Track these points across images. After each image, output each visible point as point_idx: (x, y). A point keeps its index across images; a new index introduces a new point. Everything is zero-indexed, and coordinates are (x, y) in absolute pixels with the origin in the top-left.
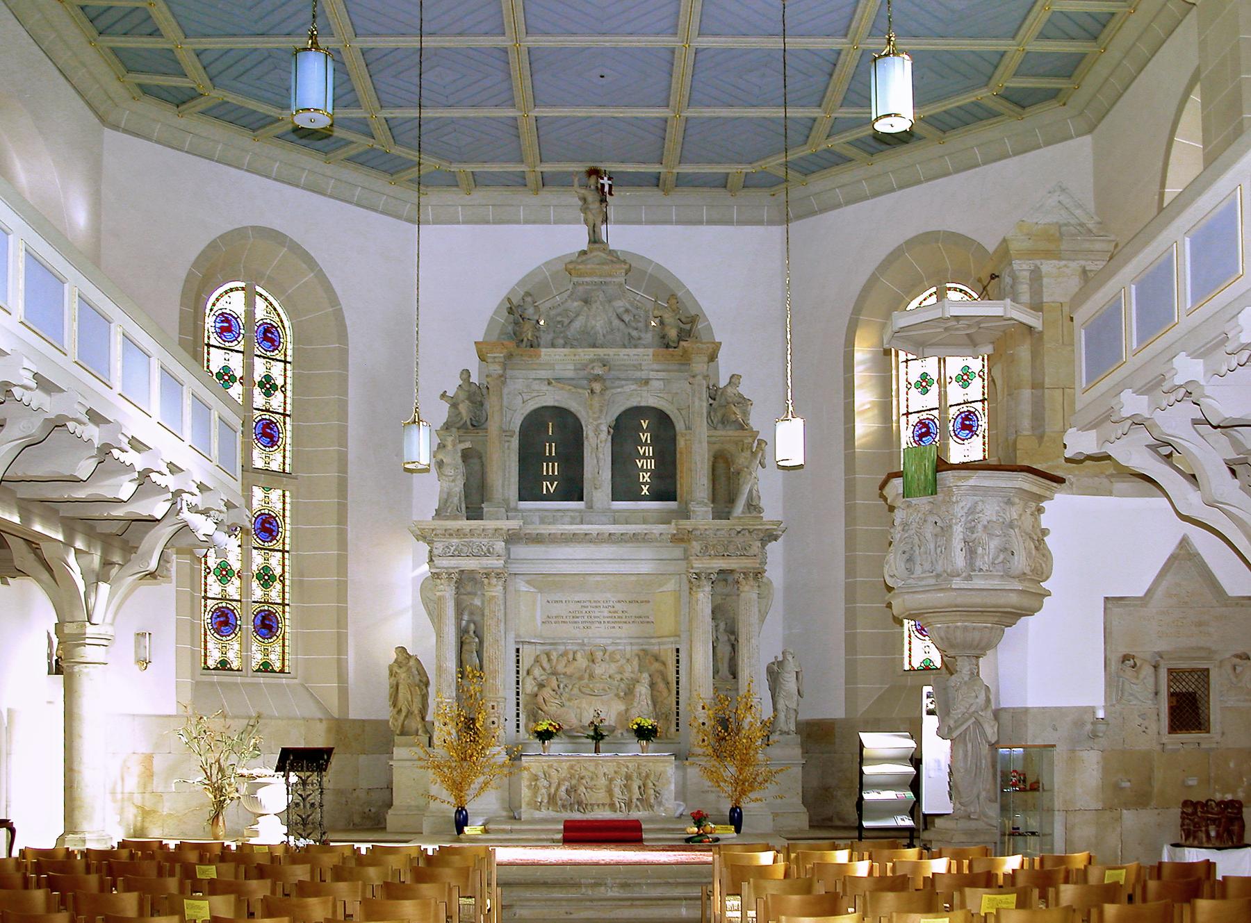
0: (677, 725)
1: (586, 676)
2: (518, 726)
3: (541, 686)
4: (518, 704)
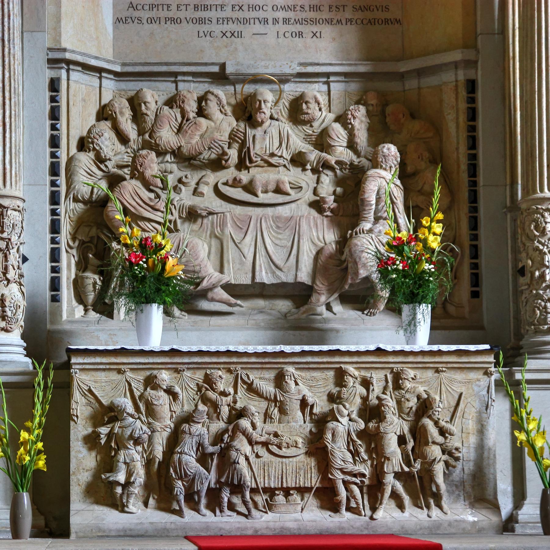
0: (476, 280)
1: (233, 154)
2: (55, 285)
3: (114, 181)
4: (55, 228)
